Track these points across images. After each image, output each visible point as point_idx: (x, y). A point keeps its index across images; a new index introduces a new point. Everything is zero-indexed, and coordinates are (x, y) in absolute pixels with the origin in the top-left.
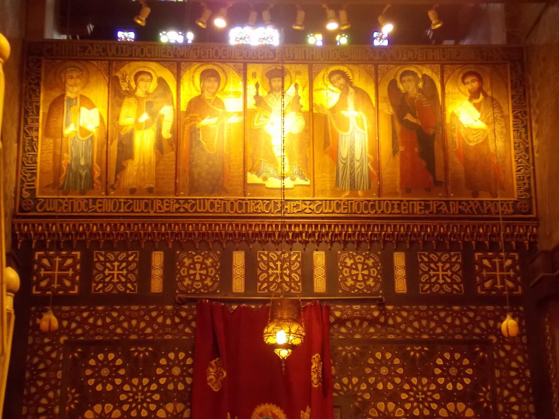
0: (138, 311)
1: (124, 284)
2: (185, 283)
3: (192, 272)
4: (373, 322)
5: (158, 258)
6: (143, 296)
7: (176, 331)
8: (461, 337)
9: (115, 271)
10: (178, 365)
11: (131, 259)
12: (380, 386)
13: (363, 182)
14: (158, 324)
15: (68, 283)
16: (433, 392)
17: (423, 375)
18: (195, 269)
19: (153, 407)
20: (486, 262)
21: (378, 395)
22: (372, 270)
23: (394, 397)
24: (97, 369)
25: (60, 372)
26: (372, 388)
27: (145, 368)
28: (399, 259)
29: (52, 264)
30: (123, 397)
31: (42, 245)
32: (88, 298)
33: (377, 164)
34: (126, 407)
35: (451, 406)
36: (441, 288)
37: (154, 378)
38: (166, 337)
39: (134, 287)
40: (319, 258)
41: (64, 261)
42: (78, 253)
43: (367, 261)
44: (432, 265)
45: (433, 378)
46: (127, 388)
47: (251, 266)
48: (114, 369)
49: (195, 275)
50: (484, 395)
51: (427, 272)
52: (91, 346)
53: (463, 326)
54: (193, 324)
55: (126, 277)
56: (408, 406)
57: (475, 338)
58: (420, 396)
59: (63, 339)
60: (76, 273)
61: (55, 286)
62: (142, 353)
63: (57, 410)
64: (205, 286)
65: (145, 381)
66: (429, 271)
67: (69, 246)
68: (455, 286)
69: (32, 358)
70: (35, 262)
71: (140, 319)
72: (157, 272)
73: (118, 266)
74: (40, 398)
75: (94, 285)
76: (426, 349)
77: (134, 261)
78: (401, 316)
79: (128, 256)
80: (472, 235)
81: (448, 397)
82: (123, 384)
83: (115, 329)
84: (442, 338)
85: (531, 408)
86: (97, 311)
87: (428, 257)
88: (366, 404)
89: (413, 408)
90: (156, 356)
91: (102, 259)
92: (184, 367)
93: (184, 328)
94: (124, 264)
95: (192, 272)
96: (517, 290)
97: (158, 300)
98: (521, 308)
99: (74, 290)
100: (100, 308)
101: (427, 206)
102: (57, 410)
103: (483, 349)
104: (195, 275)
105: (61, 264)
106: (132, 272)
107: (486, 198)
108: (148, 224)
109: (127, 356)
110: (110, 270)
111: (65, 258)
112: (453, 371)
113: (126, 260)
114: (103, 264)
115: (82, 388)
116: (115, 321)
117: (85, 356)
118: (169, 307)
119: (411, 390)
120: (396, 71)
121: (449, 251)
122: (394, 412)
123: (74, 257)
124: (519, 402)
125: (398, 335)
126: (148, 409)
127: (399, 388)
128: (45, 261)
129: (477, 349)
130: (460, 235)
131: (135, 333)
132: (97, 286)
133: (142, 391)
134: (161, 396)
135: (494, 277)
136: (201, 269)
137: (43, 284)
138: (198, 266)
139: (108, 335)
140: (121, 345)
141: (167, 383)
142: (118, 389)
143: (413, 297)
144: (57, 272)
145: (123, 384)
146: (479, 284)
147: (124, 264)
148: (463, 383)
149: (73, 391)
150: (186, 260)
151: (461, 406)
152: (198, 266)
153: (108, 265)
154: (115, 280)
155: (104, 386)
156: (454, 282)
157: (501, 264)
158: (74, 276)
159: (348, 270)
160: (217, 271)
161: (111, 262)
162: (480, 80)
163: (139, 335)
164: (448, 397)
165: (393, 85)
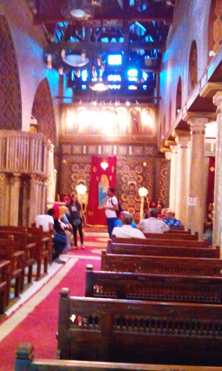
4: (125, 160)
5: (85, 147)
6: (82, 154)
13: (124, 132)
21: (124, 173)
23: (128, 174)
27: (83, 168)
31: (64, 144)
32: (72, 154)
33: (127, 129)
40: (115, 147)
45: (134, 170)
47: (102, 149)
52: (73, 163)
62: (82, 165)
88: (122, 176)
92: (89, 167)
97: (85, 155)
101: (136, 137)
107: (148, 136)
109: (79, 165)
120: (132, 109)
140: (78, 163)
143: (132, 156)
162: (149, 111)
164: (137, 174)
165: (131, 112)
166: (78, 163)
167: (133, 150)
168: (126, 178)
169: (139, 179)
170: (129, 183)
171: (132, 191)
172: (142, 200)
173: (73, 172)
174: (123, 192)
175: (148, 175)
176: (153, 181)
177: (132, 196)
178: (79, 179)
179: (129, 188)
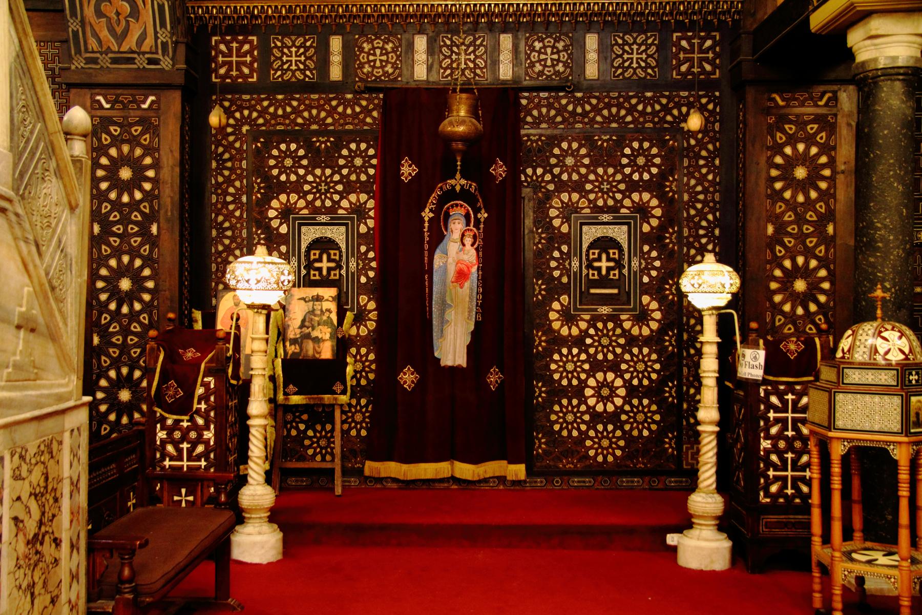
0: (318, 100)
1: (303, 71)
2: (365, 70)
3: (371, 58)
5: (336, 43)
7: (356, 121)
8: (651, 125)
9: (292, 59)
10: (360, 156)
11: (308, 44)
12: (565, 177)
14: (339, 114)
15: (246, 71)
16: (619, 182)
17: (609, 165)
18: (374, 55)
19: (336, 197)
20: (684, 43)
22: (561, 54)
23: (578, 187)
24: (280, 159)
25: (244, 162)
26: (556, 179)
28: (592, 41)
29: (230, 49)
30: (307, 187)
32: (269, 88)
34: (310, 197)
35: (635, 196)
36: (635, 73)
37: (337, 169)
38: (347, 127)
39: (313, 74)
41: (241, 47)
42: (255, 38)
43: (557, 45)
44: (627, 48)
45: (619, 168)
46: (310, 178)
48: (297, 160)
49: (375, 61)
50: (671, 186)
51: (621, 56)
52: (273, 137)
53: (655, 113)
54: (375, 114)
55: (304, 63)
56: (592, 196)
57: (666, 126)
58: (605, 187)
59: (245, 129)
60: (254, 60)
61: (234, 73)
62: (322, 143)
63: (244, 199)
64: (386, 73)
65: (328, 172)
66: (623, 54)
67: (246, 31)
68: (649, 71)
69: (217, 148)
70: (212, 48)
71: (320, 108)
72: (336, 59)
73: (296, 52)
74: (228, 187)
75: (272, 72)
76: (614, 138)
77: (311, 46)
78: (590, 104)
79: (306, 41)
80: (671, 13)
81: (633, 186)
82: (306, 175)
83: (295, 118)
84: (632, 126)
85: (717, 197)
86: (277, 100)
87: (622, 38)
88: (548, 196)
89: (596, 199)
90: (337, 146)
91: (279, 44)
92: (367, 159)
93: (365, 117)
94: (302, 50)
95: (371, 58)
96: (715, 74)
97: (337, 88)
98: (717, 94)
99: (253, 77)
100: (280, 97)
102: (244, 199)
103: (673, 138)
104: (375, 61)
105: (239, 50)
106: (310, 58)
108: (325, 6)
110: (288, 56)
111: (242, 44)
112: (641, 161)
113: (303, 45)
114: (281, 49)
115: (267, 178)
116: (296, 111)
117: (268, 146)
118: (349, 96)
119: (597, 180)
121: (645, 32)
122: (578, 202)
123: (251, 42)
124: (705, 191)
125: (586, 124)
126: (331, 199)
127: (584, 179)
128: (223, 47)
129: (668, 137)
130: (658, 13)
131: (316, 123)
132: (275, 74)
133: (325, 181)
134: (344, 187)
135: (691, 60)
136: (381, 54)
137: (222, 71)
138: (378, 52)
139: (288, 125)
140: (302, 136)
141: (349, 174)
142: (302, 180)
144: (234, 59)
145: (306, 175)
146: (675, 68)
147: (302, 50)
148: (649, 172)
149: (259, 181)
150: (365, 45)
151: (646, 196)
152: (378, 52)
153: (286, 50)
154: (294, 67)
155: (288, 176)
156: (648, 66)
157: (701, 45)
158: (252, 63)
159: (537, 54)
160: (398, 57)
161: (289, 48)
163: (320, 125)
166: (302, 136)
167: (603, 50)
168: (569, 211)
169: (643, 211)
170: (590, 233)
171: (604, 282)
172: (710, 335)
173: (274, 188)
174: (555, 289)
175: (694, 195)
176: (717, 223)
177: (605, 310)
178: (311, 222)
179: (590, 266)
